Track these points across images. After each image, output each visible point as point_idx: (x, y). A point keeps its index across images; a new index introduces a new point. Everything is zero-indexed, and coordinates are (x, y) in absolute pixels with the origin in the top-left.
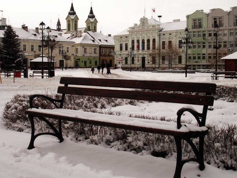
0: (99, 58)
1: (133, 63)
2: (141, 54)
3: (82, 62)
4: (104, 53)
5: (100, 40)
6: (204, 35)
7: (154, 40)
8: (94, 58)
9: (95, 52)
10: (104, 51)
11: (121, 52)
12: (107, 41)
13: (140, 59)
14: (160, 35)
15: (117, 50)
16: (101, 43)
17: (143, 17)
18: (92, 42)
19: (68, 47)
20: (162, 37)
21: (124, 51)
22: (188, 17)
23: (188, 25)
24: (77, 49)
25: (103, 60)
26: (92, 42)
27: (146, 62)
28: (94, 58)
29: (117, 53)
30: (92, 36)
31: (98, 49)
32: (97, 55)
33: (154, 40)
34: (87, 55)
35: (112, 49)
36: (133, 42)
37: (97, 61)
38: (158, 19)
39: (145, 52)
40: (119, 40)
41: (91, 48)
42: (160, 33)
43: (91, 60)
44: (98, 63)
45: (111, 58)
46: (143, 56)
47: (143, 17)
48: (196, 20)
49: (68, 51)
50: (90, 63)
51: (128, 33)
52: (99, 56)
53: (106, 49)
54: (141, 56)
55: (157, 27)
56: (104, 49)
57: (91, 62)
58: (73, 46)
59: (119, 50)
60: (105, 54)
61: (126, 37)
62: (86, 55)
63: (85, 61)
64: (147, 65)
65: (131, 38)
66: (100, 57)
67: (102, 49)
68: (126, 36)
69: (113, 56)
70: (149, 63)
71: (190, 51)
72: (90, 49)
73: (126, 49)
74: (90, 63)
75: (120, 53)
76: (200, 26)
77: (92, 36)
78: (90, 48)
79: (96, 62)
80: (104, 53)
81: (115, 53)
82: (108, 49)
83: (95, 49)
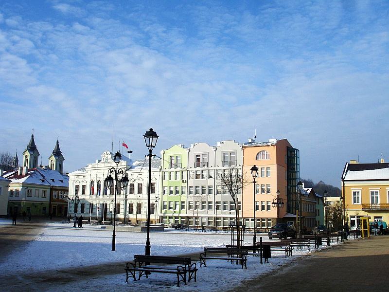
5: (53, 180)
8: (41, 204)
9: (44, 196)
12: (62, 181)
16: (53, 184)
18: (40, 182)
26: (40, 182)
30: (42, 175)
31: (48, 191)
32: (47, 199)
34: (33, 199)
36: (92, 182)
41: (39, 190)
52: (49, 201)
60: (58, 198)
62: (30, 199)
66: (50, 202)
72: (37, 191)
73: (83, 193)
77: (42, 175)
80: (57, 197)
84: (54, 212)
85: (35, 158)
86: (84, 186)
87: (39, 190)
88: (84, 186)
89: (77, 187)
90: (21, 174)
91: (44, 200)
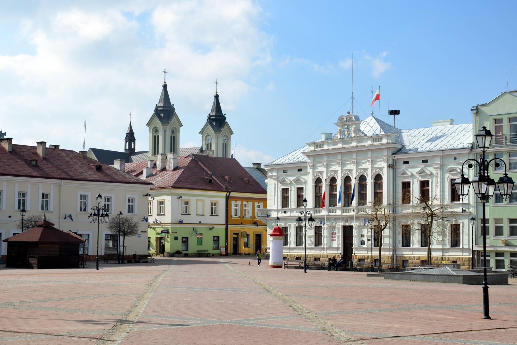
0: (224, 227)
1: (318, 242)
2: (337, 218)
3: (176, 238)
4: (239, 214)
7: (378, 178)
8: (210, 229)
9: (213, 212)
10: (239, 208)
11: (285, 212)
13: (339, 233)
15: (275, 207)
19: (131, 196)
21: (294, 210)
24: (161, 203)
25: (237, 234)
27: (355, 241)
28: (210, 229)
29: (274, 215)
32: (221, 219)
33: (378, 178)
34: (192, 218)
35: (262, 204)
36: (318, 182)
37: (218, 237)
38: (389, 119)
42: (397, 157)
43: (201, 234)
44: (222, 242)
45: (258, 229)
46: (347, 224)
49: (130, 209)
50: (200, 241)
52: (224, 223)
53: (245, 203)
54: (340, 224)
55: (385, 141)
56: (239, 203)
57: (201, 238)
58: (147, 195)
59: (280, 207)
61: (300, 170)
62: (186, 219)
63: (183, 238)
65: (311, 173)
67: (233, 203)
68: (300, 166)
69: (264, 222)
71: (493, 210)
72: (200, 204)
74: (200, 241)
75: (281, 215)
78: (200, 200)
79: (216, 239)
80: (239, 214)
81: (269, 216)
82: (251, 203)
83: (214, 204)
84: (236, 246)
85: (173, 132)
86: (300, 190)
87: (203, 201)
88: (300, 190)
89: (285, 191)
90: (164, 169)
91: (213, 220)
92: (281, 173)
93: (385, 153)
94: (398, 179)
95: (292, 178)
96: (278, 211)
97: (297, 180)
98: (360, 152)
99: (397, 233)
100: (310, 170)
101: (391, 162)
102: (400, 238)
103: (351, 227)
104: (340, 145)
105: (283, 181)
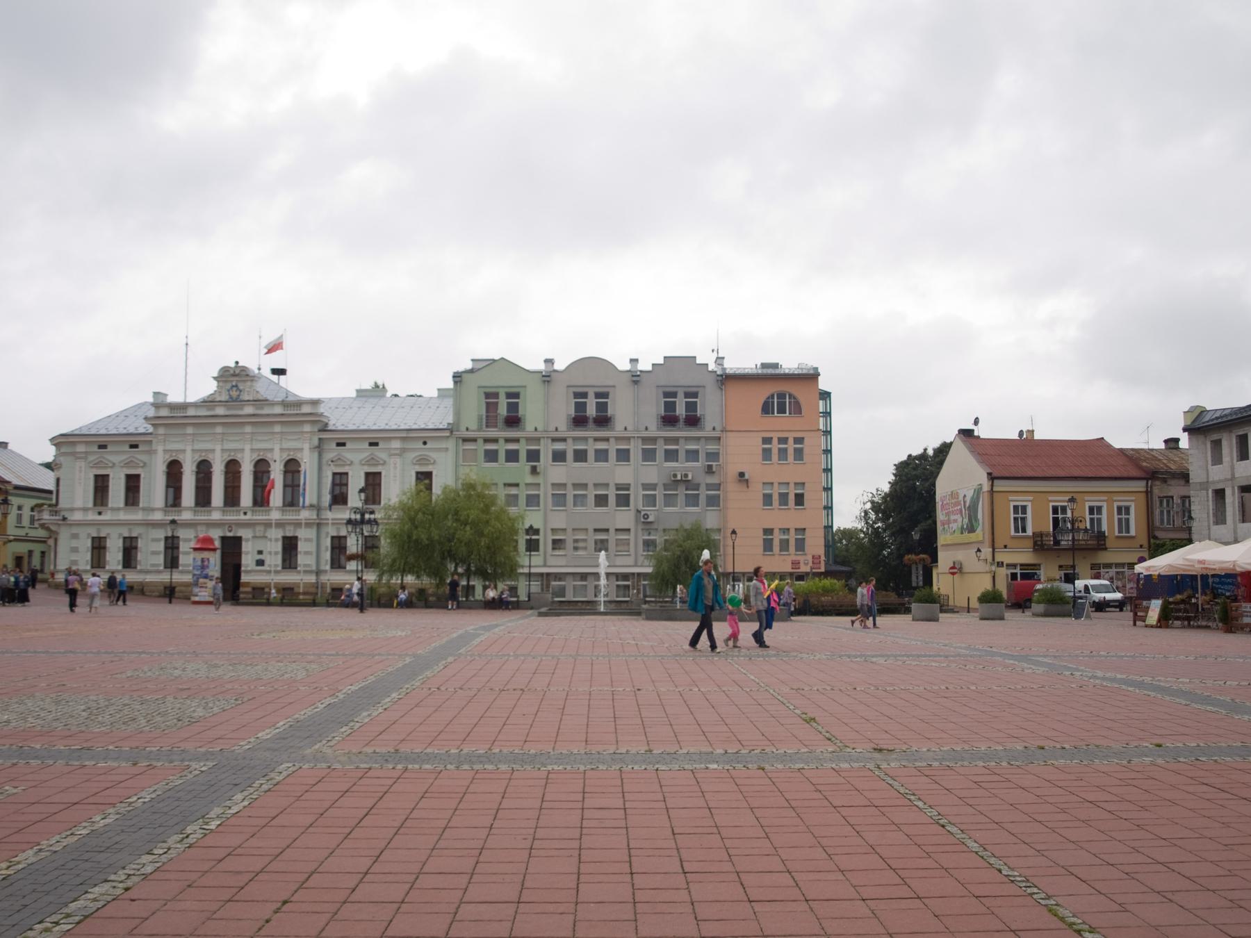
1: (172, 562)
6: (533, 456)
7: (292, 468)
11: (100, 513)
14: (319, 448)
15: (79, 503)
17: (233, 365)
20: (332, 452)
21: (119, 509)
22: (458, 377)
23: (457, 413)
27: (248, 561)
33: (292, 468)
39: (242, 517)
40: (91, 458)
47: (233, 365)
48: (496, 395)
51: (151, 429)
55: (306, 409)
59: (91, 505)
61: (132, 446)
64: (250, 576)
70: (260, 563)
75: (92, 516)
76: (513, 421)
81: (64, 519)
92: (95, 449)
93: (307, 428)
94: (324, 467)
95: (115, 459)
96: (85, 510)
97: (128, 464)
98: (262, 422)
99: (323, 548)
100: (160, 449)
101: (316, 442)
102: (327, 556)
103: (238, 540)
104: (220, 411)
105: (96, 465)
